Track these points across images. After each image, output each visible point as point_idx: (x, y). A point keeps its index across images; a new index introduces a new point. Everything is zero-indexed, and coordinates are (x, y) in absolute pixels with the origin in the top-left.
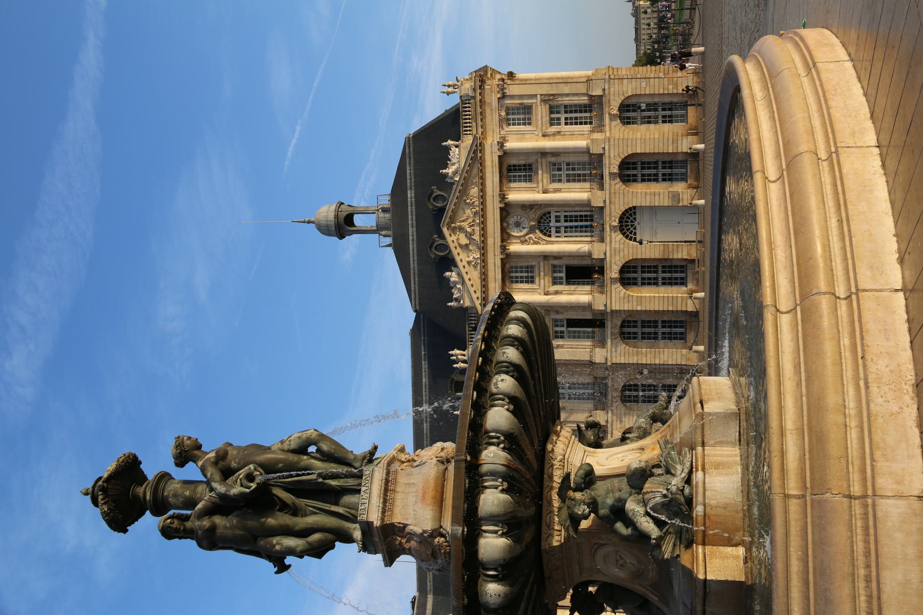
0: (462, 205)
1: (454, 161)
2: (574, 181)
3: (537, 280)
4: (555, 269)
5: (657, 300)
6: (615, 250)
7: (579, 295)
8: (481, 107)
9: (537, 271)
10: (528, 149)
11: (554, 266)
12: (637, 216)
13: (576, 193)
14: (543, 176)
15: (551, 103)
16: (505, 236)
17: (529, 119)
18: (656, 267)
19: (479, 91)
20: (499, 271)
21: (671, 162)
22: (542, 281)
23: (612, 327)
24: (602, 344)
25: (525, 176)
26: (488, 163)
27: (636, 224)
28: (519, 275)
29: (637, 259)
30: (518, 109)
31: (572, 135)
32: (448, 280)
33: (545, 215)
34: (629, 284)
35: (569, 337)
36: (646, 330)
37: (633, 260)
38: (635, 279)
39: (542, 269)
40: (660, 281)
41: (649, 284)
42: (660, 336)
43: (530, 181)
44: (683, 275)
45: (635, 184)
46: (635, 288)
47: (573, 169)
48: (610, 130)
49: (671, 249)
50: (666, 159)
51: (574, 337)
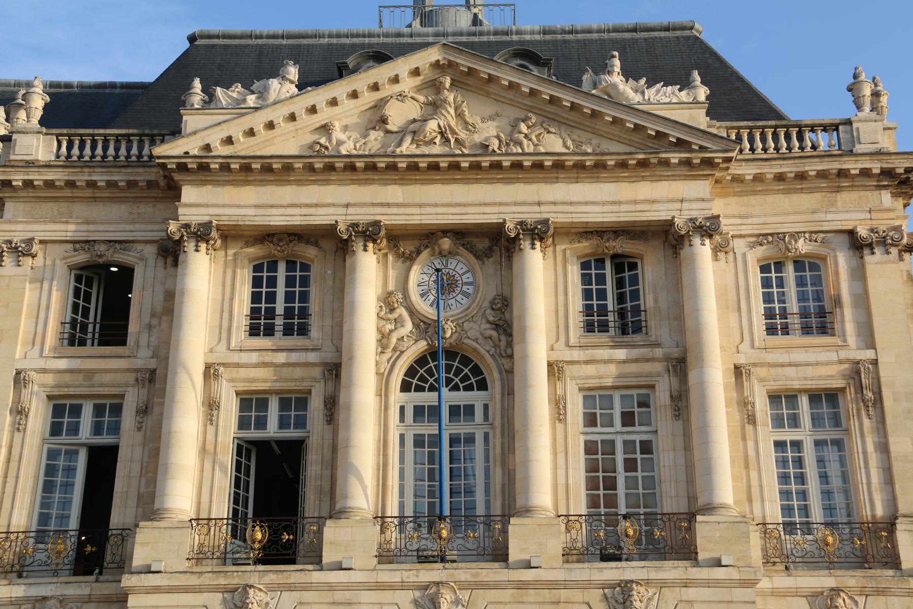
0: (513, 113)
1: (650, 93)
2: (592, 467)
3: (262, 342)
4: (294, 403)
10: (697, 310)
11: (303, 402)
13: (553, 469)
14: (608, 361)
15: (850, 394)
16: (407, 247)
17: (786, 330)
20: (294, 218)
22: (254, 358)
26: (645, 189)
28: (281, 290)
30: (818, 297)
31: (746, 463)
33: (476, 371)
39: (295, 357)
43: (589, 327)
47: (630, 465)
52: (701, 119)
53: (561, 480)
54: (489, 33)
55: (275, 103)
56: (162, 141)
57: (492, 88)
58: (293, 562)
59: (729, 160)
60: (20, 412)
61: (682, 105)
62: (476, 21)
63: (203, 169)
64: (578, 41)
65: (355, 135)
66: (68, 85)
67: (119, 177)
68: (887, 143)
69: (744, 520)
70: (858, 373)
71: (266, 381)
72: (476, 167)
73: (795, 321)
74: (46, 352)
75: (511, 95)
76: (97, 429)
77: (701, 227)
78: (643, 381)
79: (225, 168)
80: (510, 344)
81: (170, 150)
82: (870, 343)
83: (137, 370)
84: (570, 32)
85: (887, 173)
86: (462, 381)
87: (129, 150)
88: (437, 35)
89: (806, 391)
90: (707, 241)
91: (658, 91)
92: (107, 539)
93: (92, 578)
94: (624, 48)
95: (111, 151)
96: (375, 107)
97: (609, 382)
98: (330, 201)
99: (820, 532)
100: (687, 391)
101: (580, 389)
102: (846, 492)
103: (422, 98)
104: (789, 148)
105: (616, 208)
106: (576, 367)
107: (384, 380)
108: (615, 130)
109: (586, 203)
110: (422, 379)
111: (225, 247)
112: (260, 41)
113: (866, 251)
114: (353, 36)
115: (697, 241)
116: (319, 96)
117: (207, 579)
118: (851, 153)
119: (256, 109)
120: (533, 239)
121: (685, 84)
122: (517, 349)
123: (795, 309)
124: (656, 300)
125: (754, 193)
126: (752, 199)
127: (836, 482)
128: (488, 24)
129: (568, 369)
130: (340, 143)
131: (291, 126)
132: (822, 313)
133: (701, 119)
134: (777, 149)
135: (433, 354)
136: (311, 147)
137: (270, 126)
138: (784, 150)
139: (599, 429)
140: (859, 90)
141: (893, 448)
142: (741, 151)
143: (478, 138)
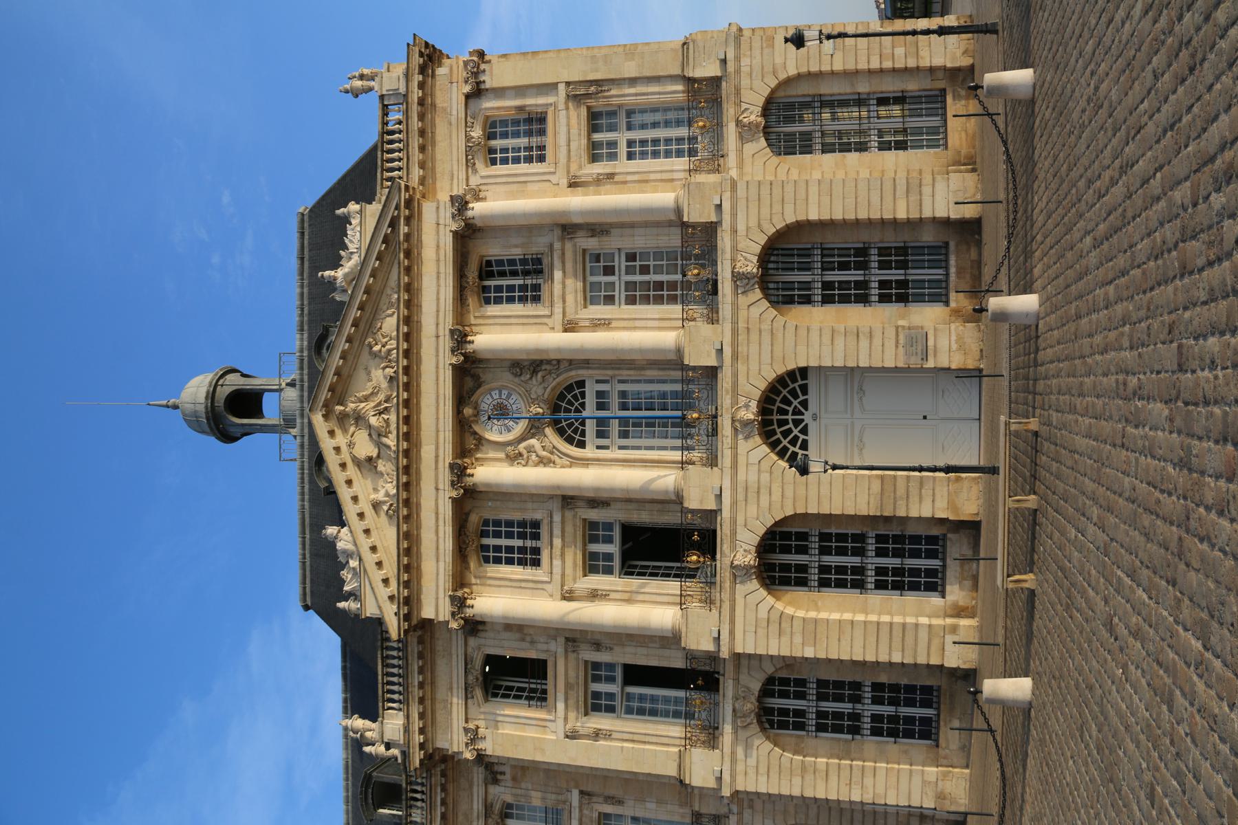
1: (352, 247)
2: (646, 300)
3: (545, 556)
4: (593, 532)
5: (858, 633)
6: (747, 490)
7: (647, 607)
8: (422, 117)
9: (544, 531)
10: (525, 215)
11: (593, 525)
12: (812, 397)
13: (646, 330)
14: (564, 285)
16: (471, 443)
17: (542, 148)
18: (861, 538)
19: (417, 78)
20: (447, 531)
21: (903, 250)
22: (557, 563)
23: (734, 696)
24: (711, 735)
25: (523, 288)
27: (807, 417)
28: (503, 542)
29: (805, 516)
30: (516, 122)
31: (644, 182)
32: (331, 544)
33: (569, 388)
34: (786, 582)
35: (629, 711)
36: (829, 706)
37: (795, 516)
38: (803, 568)
39: (557, 531)
40: (871, 578)
41: (841, 584)
42: (867, 724)
43: (537, 299)
44: (934, 563)
45: (805, 309)
46: (800, 594)
47: (645, 270)
48: (741, 164)
49: (901, 491)
50: (891, 239)
51: (641, 712)
52: (374, 209)
53: (656, 324)
54: (302, 374)
55: (355, 544)
56: (387, 632)
57: (345, 372)
58: (715, 531)
59: (407, 187)
60: (597, 735)
61: (362, 223)
62: (292, 384)
63: (409, 602)
64: (310, 304)
65: (381, 482)
66: (345, 701)
67: (415, 665)
68: (399, 69)
69: (687, 186)
70: (576, 96)
71: (575, 554)
72: (407, 387)
73: (535, 141)
74: (551, 717)
75: (350, 358)
76: (611, 679)
77: (459, 210)
78: (580, 259)
79: (407, 584)
80: (549, 362)
81: (393, 626)
82: (554, 86)
83: (566, 651)
84: (302, 310)
85: (423, 70)
86: (577, 400)
87: (394, 658)
88: (302, 416)
89: (589, 135)
90: (471, 205)
91: (351, 241)
92: (693, 670)
93: (721, 679)
94: (316, 267)
95: (395, 671)
96: (359, 467)
97: (580, 285)
98: (433, 503)
99: (695, 130)
100: (588, 224)
101: (585, 307)
102: (666, 110)
103: (352, 429)
104: (400, 141)
105: (442, 276)
106: (568, 310)
107: (576, 462)
108: (380, 276)
109: (438, 299)
110: (575, 431)
111: (469, 585)
112: (308, 556)
113: (482, 87)
114: (303, 482)
115: (470, 213)
116: (350, 511)
117: (726, 596)
118: (406, 96)
119: (360, 560)
120: (466, 342)
121: (346, 220)
122: (553, 357)
123: (526, 140)
124: (516, 246)
125: (433, 168)
126: (439, 170)
127: (658, 117)
128: (295, 375)
129: (570, 316)
130: (387, 494)
131: (373, 533)
132: (529, 120)
133: (374, 209)
134: (400, 150)
135: (555, 423)
136: (390, 517)
137: (374, 549)
138: (401, 145)
139: (616, 293)
140: (357, 89)
141: (633, 75)
142: (400, 178)
143: (384, 385)
